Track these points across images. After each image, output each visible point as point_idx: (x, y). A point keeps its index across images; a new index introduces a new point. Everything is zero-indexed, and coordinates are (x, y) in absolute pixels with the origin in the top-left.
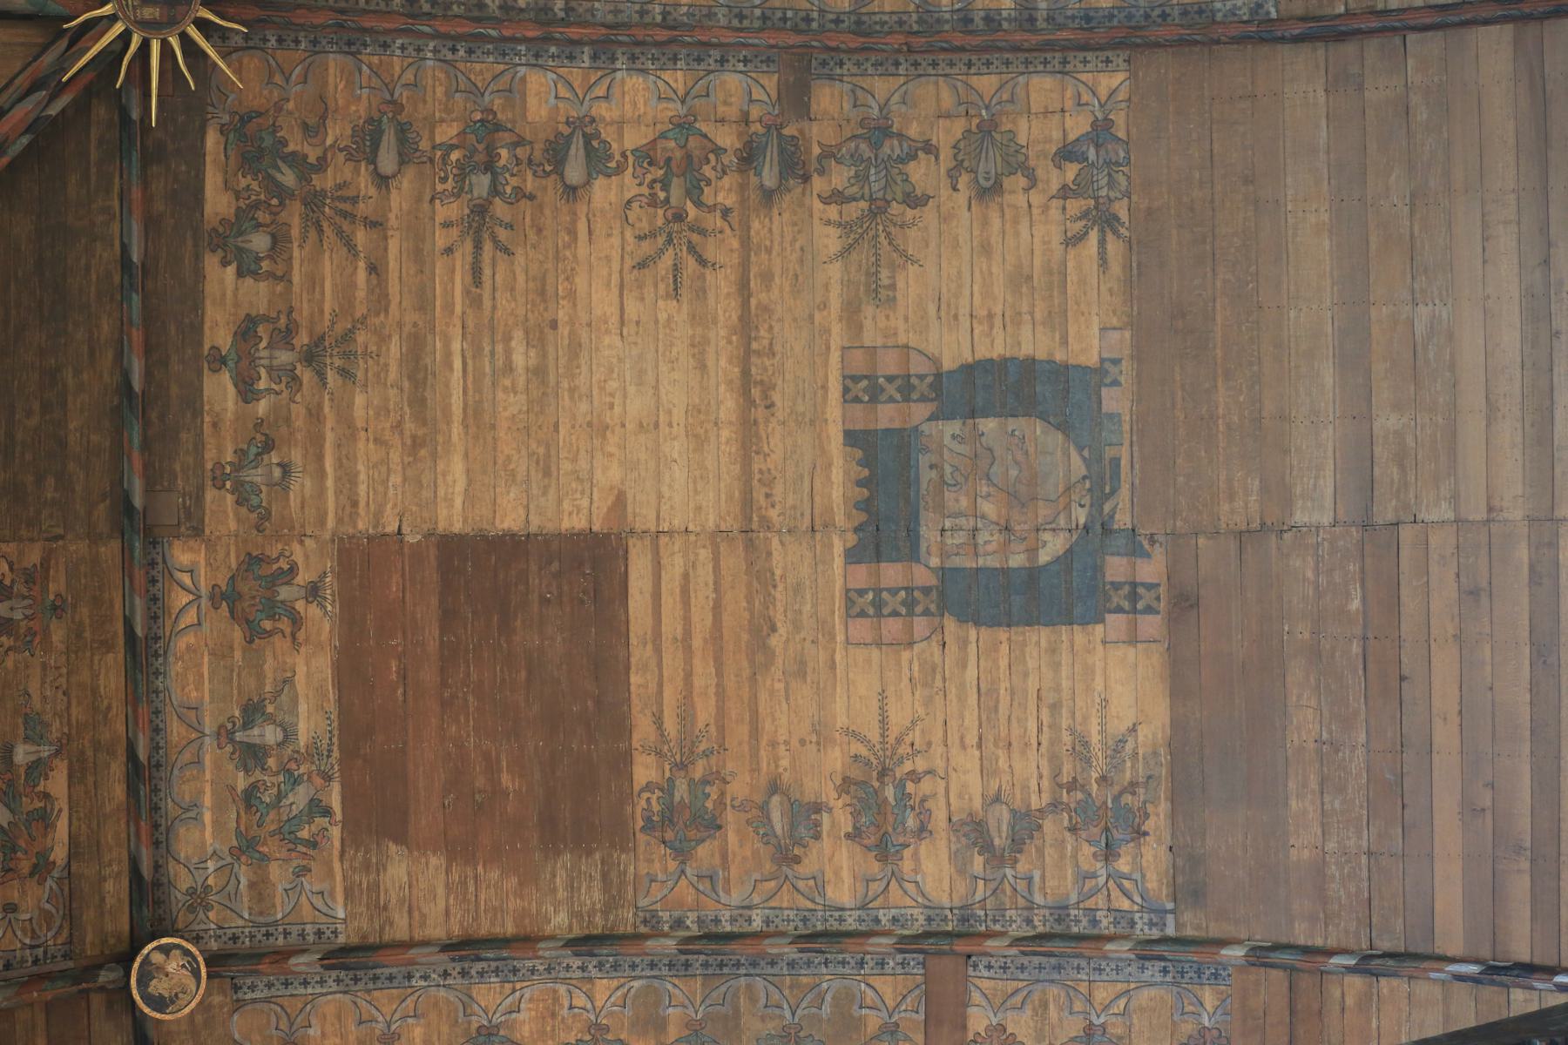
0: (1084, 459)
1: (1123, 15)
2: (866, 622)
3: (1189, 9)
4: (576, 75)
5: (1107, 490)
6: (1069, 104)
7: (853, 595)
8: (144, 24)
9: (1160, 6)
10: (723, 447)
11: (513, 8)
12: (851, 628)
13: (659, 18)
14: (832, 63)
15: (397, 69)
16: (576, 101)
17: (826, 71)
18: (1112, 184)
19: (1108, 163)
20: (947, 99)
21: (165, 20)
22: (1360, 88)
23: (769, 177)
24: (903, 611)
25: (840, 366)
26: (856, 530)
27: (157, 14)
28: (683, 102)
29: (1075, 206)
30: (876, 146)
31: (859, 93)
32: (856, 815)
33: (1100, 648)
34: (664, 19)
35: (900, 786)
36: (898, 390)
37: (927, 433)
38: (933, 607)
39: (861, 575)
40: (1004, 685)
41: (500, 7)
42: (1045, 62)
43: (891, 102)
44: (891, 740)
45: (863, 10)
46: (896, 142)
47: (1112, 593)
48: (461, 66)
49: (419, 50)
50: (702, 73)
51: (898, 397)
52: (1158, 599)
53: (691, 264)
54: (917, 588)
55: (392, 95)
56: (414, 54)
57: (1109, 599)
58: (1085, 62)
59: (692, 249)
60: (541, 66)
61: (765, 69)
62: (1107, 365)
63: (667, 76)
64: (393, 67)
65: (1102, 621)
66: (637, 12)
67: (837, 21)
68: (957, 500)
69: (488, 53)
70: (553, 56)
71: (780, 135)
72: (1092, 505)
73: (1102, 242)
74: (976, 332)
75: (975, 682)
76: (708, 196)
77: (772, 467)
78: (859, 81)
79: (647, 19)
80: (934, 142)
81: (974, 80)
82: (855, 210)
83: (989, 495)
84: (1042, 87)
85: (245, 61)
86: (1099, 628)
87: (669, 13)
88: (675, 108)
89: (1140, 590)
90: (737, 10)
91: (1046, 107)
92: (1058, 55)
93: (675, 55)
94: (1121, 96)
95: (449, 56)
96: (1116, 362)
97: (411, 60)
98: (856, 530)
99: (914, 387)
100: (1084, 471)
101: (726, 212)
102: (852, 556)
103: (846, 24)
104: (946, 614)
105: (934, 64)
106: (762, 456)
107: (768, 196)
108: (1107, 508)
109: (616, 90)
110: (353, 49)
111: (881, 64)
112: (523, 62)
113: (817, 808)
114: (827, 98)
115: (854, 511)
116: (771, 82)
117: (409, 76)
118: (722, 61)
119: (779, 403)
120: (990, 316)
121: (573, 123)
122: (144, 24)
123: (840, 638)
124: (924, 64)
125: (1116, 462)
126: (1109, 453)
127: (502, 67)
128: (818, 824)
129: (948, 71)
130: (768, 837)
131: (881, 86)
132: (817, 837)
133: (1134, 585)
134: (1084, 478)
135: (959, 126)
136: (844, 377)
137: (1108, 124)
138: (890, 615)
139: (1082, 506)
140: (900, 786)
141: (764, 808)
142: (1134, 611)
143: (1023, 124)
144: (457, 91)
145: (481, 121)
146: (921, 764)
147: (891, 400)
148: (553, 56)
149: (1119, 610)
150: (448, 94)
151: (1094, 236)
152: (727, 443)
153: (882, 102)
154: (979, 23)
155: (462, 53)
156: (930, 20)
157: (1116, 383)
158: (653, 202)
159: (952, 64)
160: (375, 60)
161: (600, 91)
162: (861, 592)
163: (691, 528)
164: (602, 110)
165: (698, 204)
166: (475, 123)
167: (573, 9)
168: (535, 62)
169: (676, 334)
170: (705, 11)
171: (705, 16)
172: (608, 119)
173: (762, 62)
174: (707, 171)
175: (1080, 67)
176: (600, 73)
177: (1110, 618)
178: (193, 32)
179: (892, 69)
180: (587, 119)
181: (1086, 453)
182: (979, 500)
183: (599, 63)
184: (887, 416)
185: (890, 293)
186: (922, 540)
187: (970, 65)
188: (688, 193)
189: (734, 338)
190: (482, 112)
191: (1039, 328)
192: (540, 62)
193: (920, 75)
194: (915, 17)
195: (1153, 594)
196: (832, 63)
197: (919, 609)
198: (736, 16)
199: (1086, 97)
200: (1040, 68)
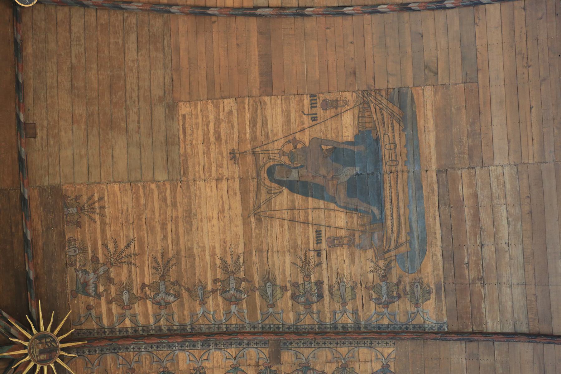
1: (392, 327)
3: (416, 326)
4: (196, 352)
6: (373, 358)
8: (41, 362)
9: (405, 324)
11: (172, 330)
13: (225, 330)
14: (288, 344)
15: (132, 357)
16: (197, 361)
17: (286, 346)
20: (330, 356)
21: (48, 358)
22: (478, 359)
27: (45, 357)
28: (235, 360)
31: (298, 354)
34: (227, 330)
41: (167, 330)
42: (365, 343)
43: (309, 357)
45: (298, 324)
46: (312, 372)
48: (155, 353)
49: (139, 349)
50: (241, 349)
55: (131, 366)
56: (137, 350)
58: (379, 343)
60: (183, 350)
61: (264, 346)
63: (228, 350)
64: (130, 356)
66: (217, 328)
67: (289, 328)
69: (164, 347)
70: (187, 346)
71: (270, 370)
78: (298, 350)
79: (221, 330)
80: (326, 371)
81: (339, 349)
84: (364, 352)
85: (77, 361)
87: (228, 327)
88: (232, 362)
90: (253, 325)
91: (365, 360)
92: (369, 341)
93: (231, 343)
94: (393, 356)
95: (150, 350)
97: (136, 353)
103: (292, 329)
105: (325, 343)
109: (211, 357)
110: (116, 351)
111: (305, 344)
112: (177, 349)
114: (287, 356)
116: (266, 351)
117: (136, 358)
118: (248, 344)
121: (196, 369)
122: (41, 362)
124: (321, 343)
127: (169, 351)
129: (330, 346)
131: (306, 352)
135: (334, 366)
137: (388, 366)
143: (357, 365)
144: (154, 362)
145: (163, 371)
148: (187, 346)
150: (151, 364)
153: (306, 357)
154: (340, 329)
155: (155, 348)
156: (323, 328)
159: (331, 344)
160: (124, 354)
161: (205, 357)
164: (206, 364)
166: (161, 372)
167: (194, 328)
168: (181, 349)
170: (241, 326)
171: (241, 328)
172: (208, 367)
173: (262, 344)
175: (377, 345)
176: (204, 351)
178: (59, 361)
179: (309, 345)
180: (201, 368)
183: (204, 347)
187: (337, 344)
190: (163, 368)
192: (183, 348)
193: (320, 348)
194: (317, 326)
196: (288, 344)
198: (252, 327)
199: (379, 356)
200: (363, 345)
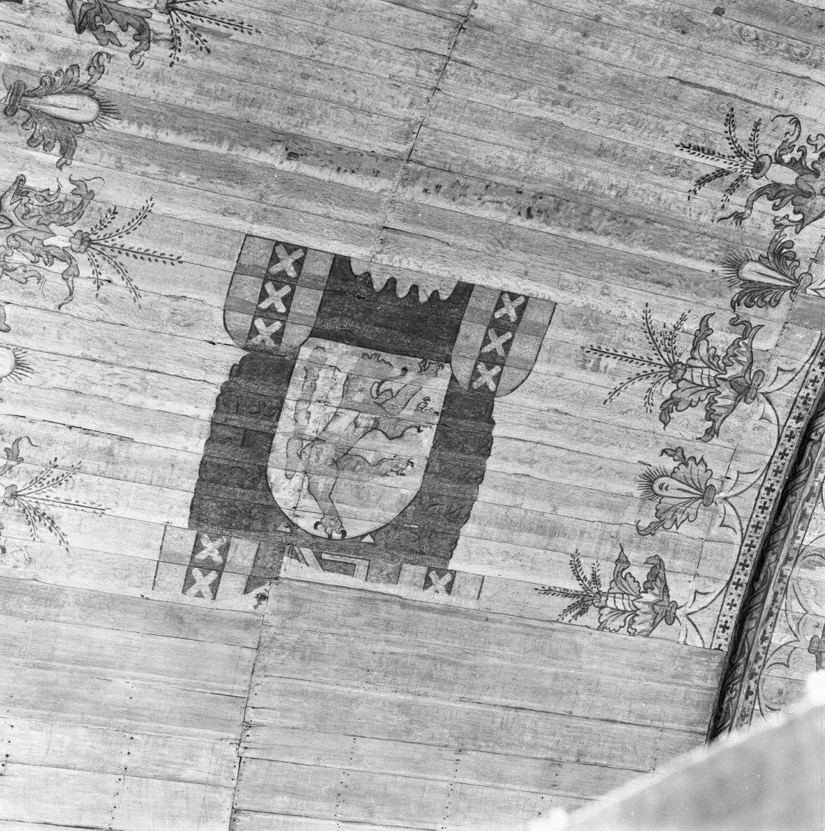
0: (363, 536)
1: (761, 651)
2: (264, 262)
5: (325, 556)
7: (298, 255)
9: (757, 691)
10: (508, 153)
12: (263, 244)
18: (617, 612)
19: (634, 613)
23: (751, 271)
24: (264, 305)
25: (540, 296)
26: (368, 274)
29: (606, 572)
30: (732, 383)
31: (790, 376)
32: (45, 195)
33: (164, 519)
35: (66, 257)
36: (494, 351)
37: (440, 372)
38: (256, 340)
39: (319, 269)
40: (151, 403)
43: (768, 407)
44: (122, 258)
46: (730, 402)
47: (219, 543)
51: (487, 349)
52: (200, 595)
53: (706, 165)
54: (283, 327)
57: (212, 539)
58: (732, 605)
59: (721, 173)
62: (448, 578)
65: (190, 528)
68: (361, 390)
71: (785, 289)
72: (314, 536)
73: (565, 593)
74: (521, 444)
75: (160, 369)
76: (763, 205)
77: (467, 200)
80: (715, 440)
82: (683, 345)
83: (357, 426)
86: (184, 522)
89: (213, 576)
92: (746, 579)
96: (449, 588)
98: (368, 274)
99: (489, 368)
100: (351, 533)
101: (739, 217)
102: (341, 265)
104: (245, 353)
106: (481, 191)
107: (735, 265)
108: (307, 552)
111: (805, 403)
113: (67, 151)
115: (388, 277)
119: (528, 223)
120: (532, 463)
123: (257, 229)
124: (788, 445)
125: (348, 569)
126: (361, 566)
128: (47, 147)
129: (773, 467)
130: (49, 86)
132: (31, 142)
133: (220, 570)
134: (344, 533)
136: (527, 298)
138: (263, 289)
139: (316, 526)
140: (66, 257)
141: (87, 90)
142: (193, 564)
146: (84, 285)
147: (486, 341)
149: (197, 547)
151: (575, 586)
152: (511, 158)
153: (772, 397)
157: (428, 583)
158: (787, 147)
162: (299, 264)
163: (439, 95)
165: (760, 193)
169: (645, 133)
174: (788, 210)
177: (190, 537)
179: (796, 413)
181: (368, 539)
182: (355, 414)
184: (471, 333)
185: (590, 365)
186: (333, 343)
188: (776, 185)
189: (613, 193)
191: (502, 511)
193: (779, 439)
195: (207, 590)
197: (260, 324)
200: (741, 560)
